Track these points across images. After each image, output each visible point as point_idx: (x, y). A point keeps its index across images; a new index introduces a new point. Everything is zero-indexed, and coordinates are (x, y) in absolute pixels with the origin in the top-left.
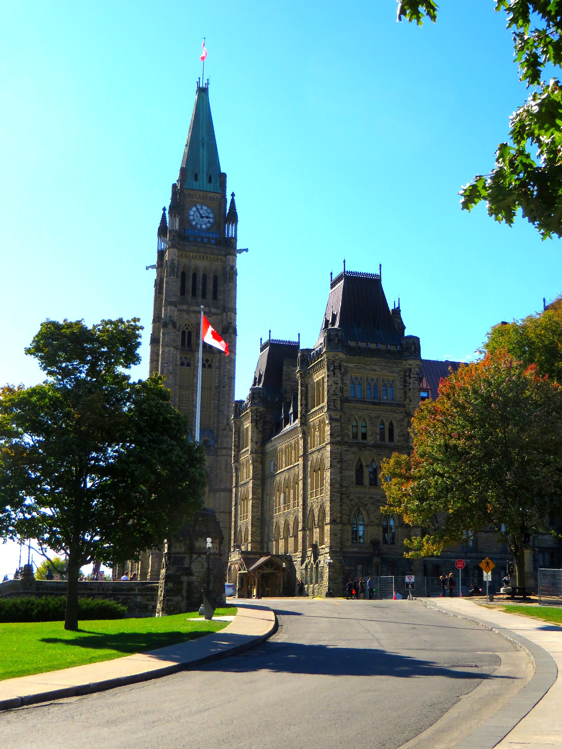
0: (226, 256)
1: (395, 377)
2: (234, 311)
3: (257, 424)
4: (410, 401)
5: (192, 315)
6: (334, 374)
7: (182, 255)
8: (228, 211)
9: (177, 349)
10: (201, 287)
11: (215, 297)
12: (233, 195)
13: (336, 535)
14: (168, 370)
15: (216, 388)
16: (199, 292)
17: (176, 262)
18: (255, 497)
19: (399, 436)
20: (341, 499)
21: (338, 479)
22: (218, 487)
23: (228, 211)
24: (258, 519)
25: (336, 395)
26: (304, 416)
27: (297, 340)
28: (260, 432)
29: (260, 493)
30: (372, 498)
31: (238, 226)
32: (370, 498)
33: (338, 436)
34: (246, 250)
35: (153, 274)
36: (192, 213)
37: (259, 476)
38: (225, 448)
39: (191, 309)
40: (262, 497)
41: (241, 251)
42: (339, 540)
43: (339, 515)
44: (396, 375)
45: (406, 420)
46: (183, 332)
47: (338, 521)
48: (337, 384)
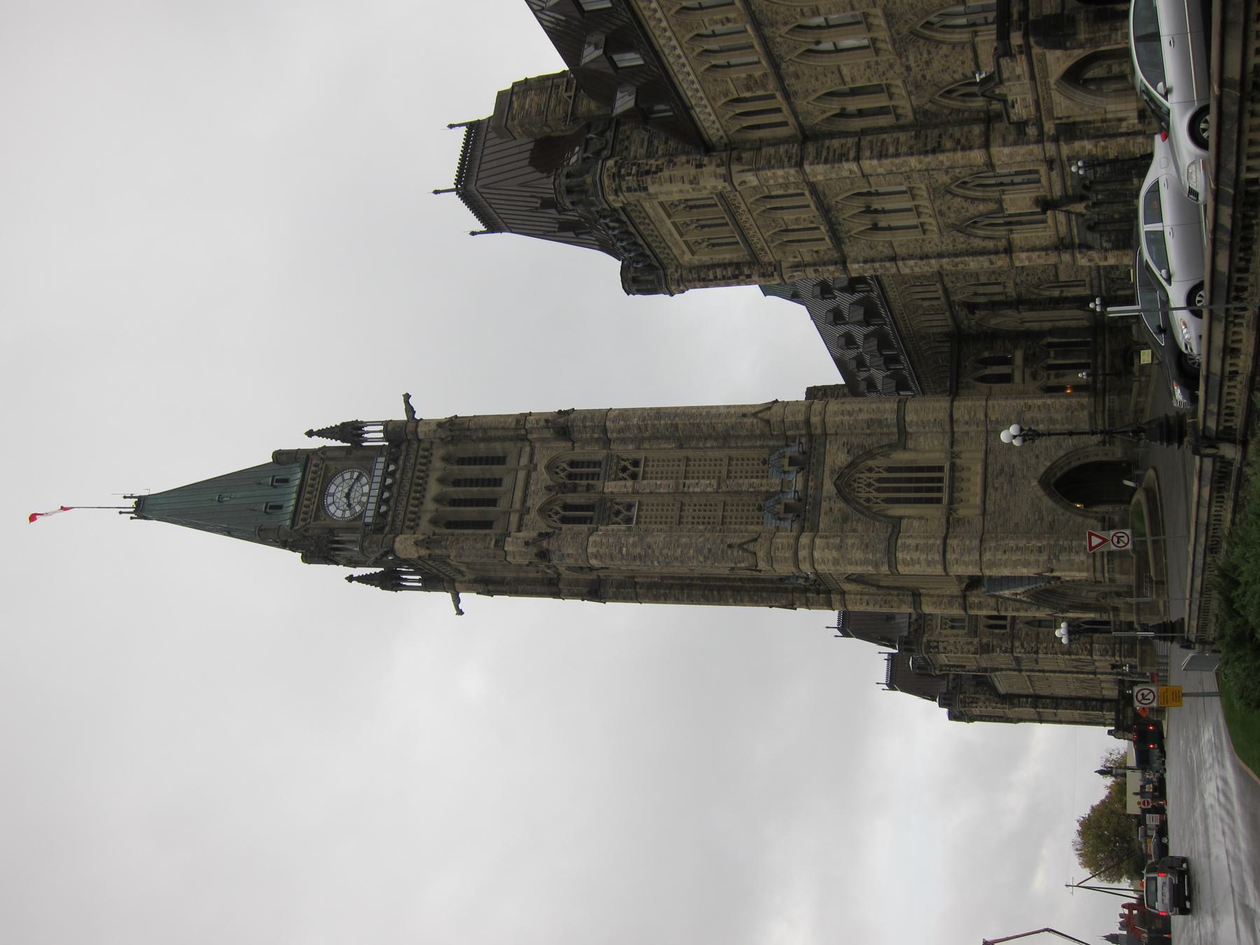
0: (420, 441)
3: (648, 172)
5: (529, 503)
8: (339, 443)
10: (475, 489)
12: (310, 434)
14: (634, 545)
15: (681, 447)
16: (486, 491)
17: (421, 537)
22: (895, 430)
23: (339, 443)
27: (464, 128)
28: (670, 161)
29: (843, 141)
34: (407, 397)
35: (469, 599)
36: (339, 513)
37: (795, 149)
39: (517, 505)
40: (855, 134)
41: (410, 410)
46: (565, 520)
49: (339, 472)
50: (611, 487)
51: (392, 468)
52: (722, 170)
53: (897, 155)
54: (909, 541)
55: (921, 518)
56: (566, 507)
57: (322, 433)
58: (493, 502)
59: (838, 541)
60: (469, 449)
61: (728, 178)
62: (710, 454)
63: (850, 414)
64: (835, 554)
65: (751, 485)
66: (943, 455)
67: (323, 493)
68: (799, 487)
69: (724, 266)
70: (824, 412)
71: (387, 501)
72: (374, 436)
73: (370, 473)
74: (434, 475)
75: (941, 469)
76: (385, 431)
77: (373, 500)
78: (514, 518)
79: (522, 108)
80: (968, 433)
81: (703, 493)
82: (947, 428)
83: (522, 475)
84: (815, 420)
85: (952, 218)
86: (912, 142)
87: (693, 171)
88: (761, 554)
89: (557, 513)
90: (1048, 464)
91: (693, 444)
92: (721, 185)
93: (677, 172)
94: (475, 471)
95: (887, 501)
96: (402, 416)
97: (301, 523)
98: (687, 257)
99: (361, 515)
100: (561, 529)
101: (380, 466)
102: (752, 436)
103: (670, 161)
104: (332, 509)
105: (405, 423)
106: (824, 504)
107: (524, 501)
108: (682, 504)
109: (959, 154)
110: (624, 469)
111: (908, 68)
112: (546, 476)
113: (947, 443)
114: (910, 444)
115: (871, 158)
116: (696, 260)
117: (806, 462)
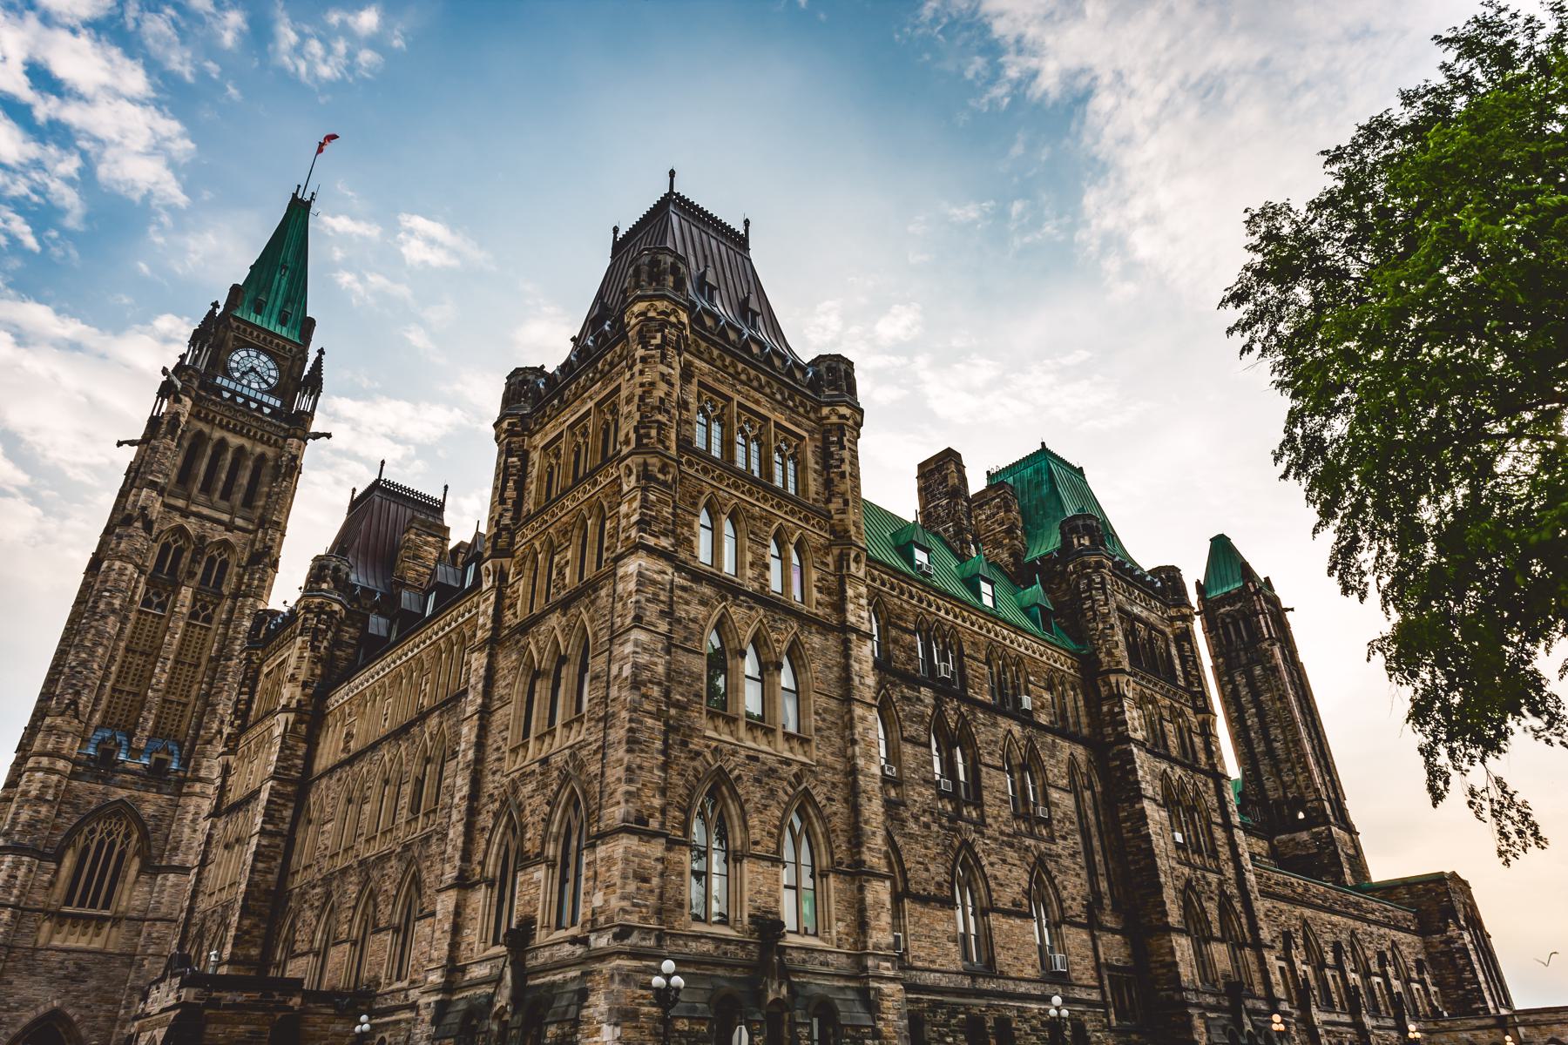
1: (802, 438)
2: (281, 528)
3: (314, 638)
4: (846, 503)
5: (192, 519)
6: (664, 356)
7: (199, 412)
9: (142, 572)
10: (223, 476)
11: (248, 502)
12: (321, 352)
13: (646, 880)
14: (109, 604)
15: (211, 659)
17: (183, 420)
18: (269, 827)
19: (820, 590)
20: (665, 742)
21: (660, 669)
24: (267, 892)
25: (668, 412)
26: (506, 527)
30: (756, 759)
31: (320, 400)
32: (748, 757)
33: (666, 536)
34: (329, 436)
35: (130, 453)
38: (200, 780)
39: (194, 508)
41: (317, 436)
42: (652, 901)
43: (657, 802)
44: (805, 434)
45: (836, 551)
46: (165, 548)
47: (654, 824)
48: (671, 385)
49: (279, 368)
50: (186, 593)
51: (267, 410)
52: (294, 704)
53: (252, 871)
54: (23, 869)
55: (52, 884)
56: (180, 552)
57: (318, 361)
58: (207, 488)
59: (49, 797)
60: (265, 478)
61: (286, 709)
62: (196, 687)
63: (193, 821)
64: (34, 793)
65: (146, 720)
66: (121, 909)
67: (261, 350)
68: (131, 766)
69: (249, 703)
70: (203, 795)
71: (233, 398)
72: (303, 403)
73: (271, 392)
74: (248, 444)
75: (106, 906)
76: (304, 412)
77: (239, 388)
78: (180, 503)
79: (427, 543)
80: (139, 934)
81: (152, 675)
82: (150, 915)
83: (226, 517)
84: (198, 787)
85: (208, 924)
86: (263, 886)
87: (301, 678)
88: (59, 721)
89: (175, 541)
90: (75, 1018)
91: (209, 673)
92: (283, 701)
93: (305, 666)
94: (244, 479)
95: (86, 849)
96: (316, 427)
97: (235, 324)
98: (265, 670)
99: (227, 374)
100: (155, 541)
101: (272, 401)
102: (199, 726)
103: (320, 659)
104: (243, 353)
105: (306, 430)
106: (101, 787)
107: (198, 515)
108: (148, 655)
109: (232, 932)
110: (204, 608)
111: (314, 887)
112: (217, 538)
113: (134, 914)
114: (143, 878)
115: (258, 845)
116: (262, 677)
117: (156, 776)
